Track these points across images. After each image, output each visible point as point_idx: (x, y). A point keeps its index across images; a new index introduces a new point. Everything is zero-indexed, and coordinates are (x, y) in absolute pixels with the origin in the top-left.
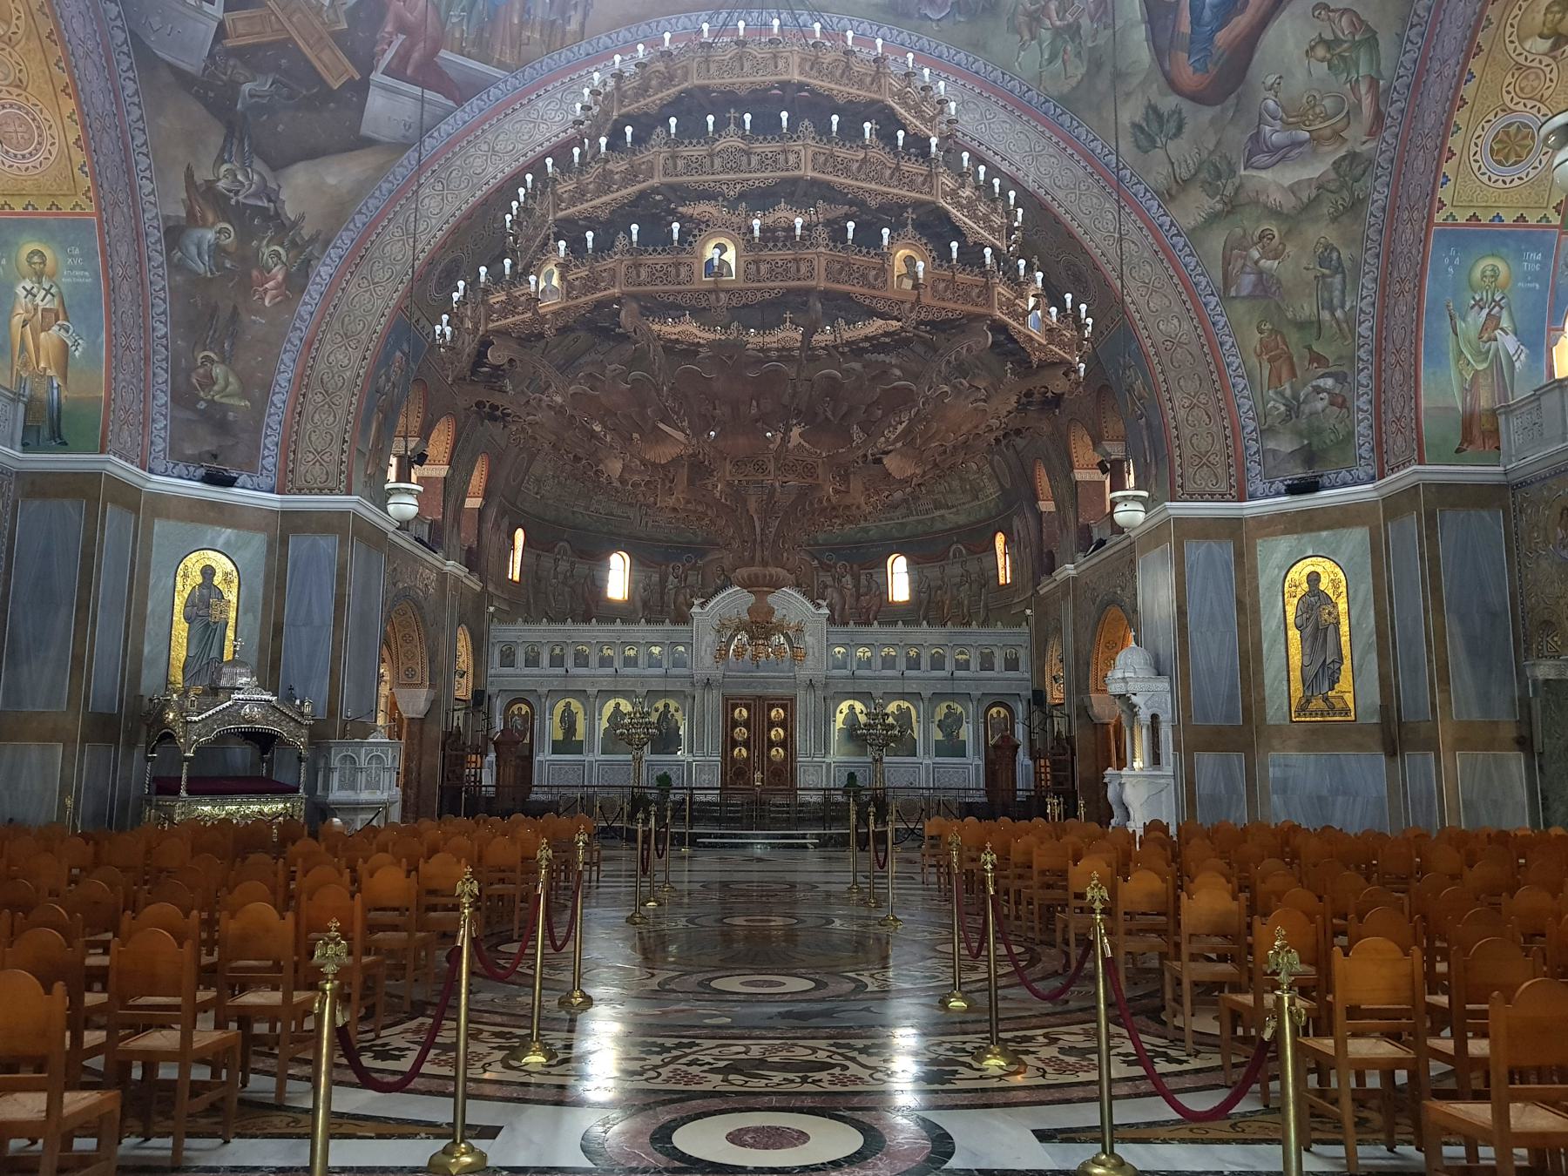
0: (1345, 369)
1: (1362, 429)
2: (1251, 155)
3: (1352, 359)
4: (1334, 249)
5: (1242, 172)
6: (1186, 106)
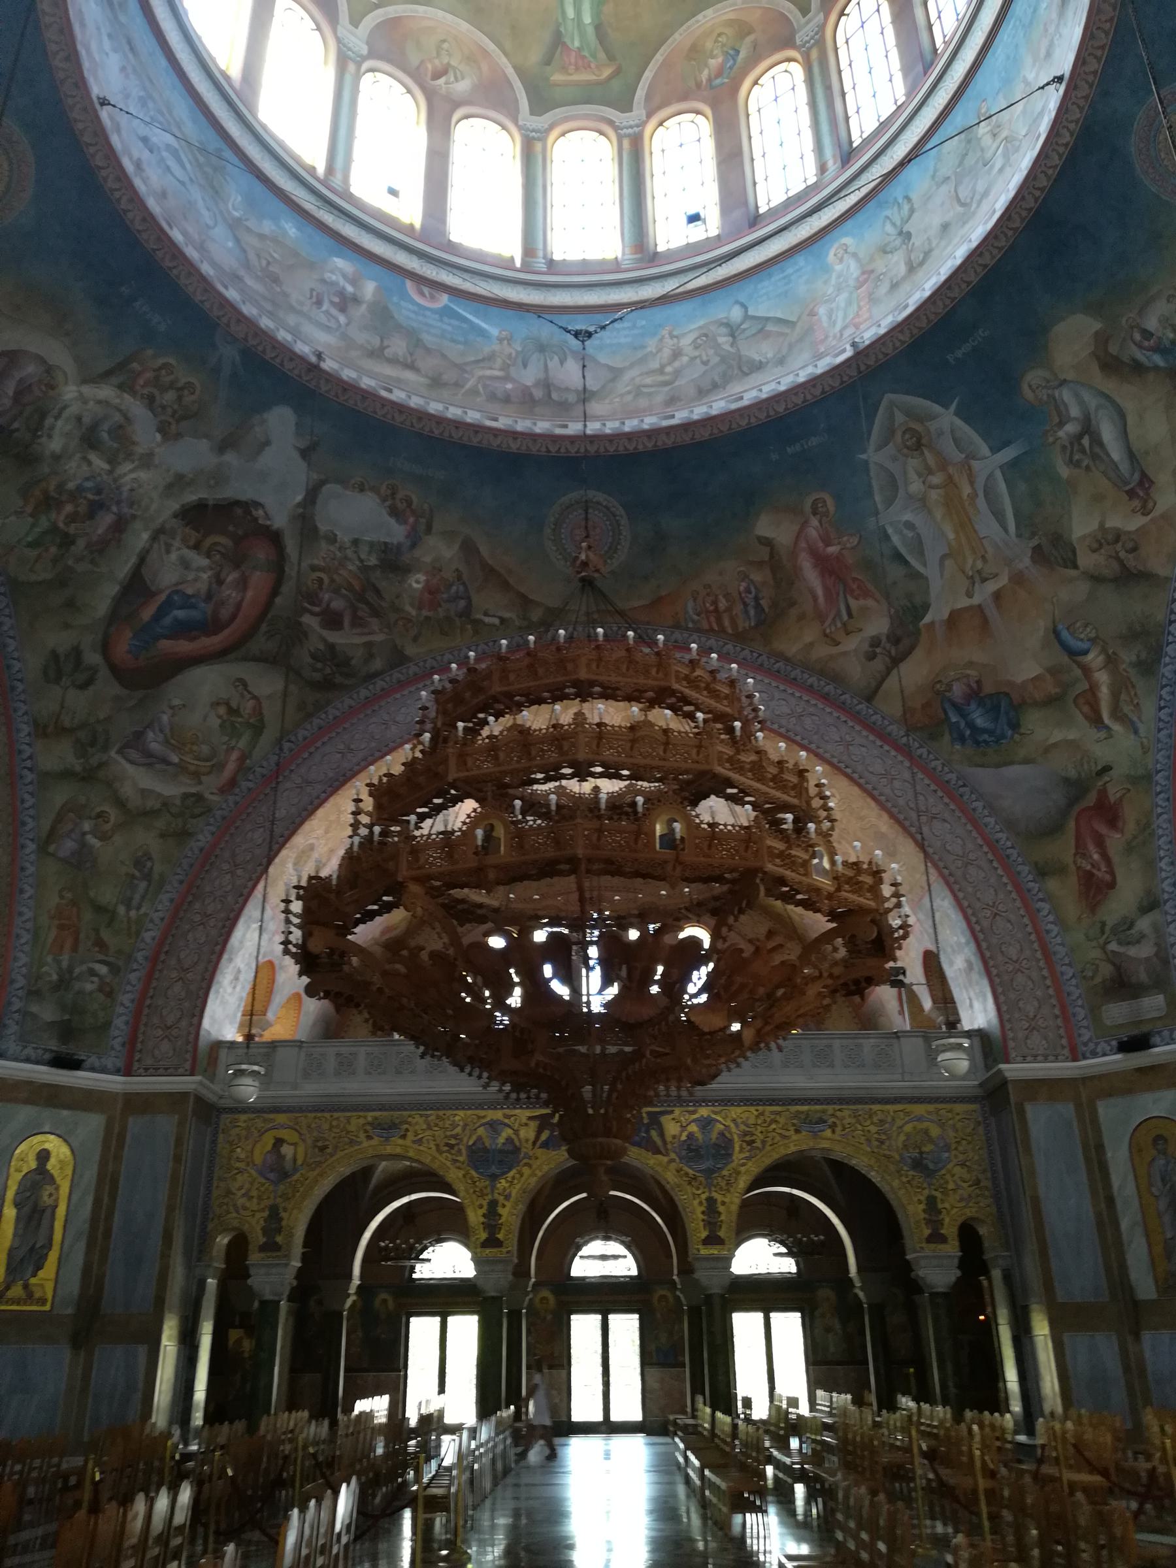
2: (127, 746)
4: (150, 859)
5: (113, 754)
6: (104, 672)
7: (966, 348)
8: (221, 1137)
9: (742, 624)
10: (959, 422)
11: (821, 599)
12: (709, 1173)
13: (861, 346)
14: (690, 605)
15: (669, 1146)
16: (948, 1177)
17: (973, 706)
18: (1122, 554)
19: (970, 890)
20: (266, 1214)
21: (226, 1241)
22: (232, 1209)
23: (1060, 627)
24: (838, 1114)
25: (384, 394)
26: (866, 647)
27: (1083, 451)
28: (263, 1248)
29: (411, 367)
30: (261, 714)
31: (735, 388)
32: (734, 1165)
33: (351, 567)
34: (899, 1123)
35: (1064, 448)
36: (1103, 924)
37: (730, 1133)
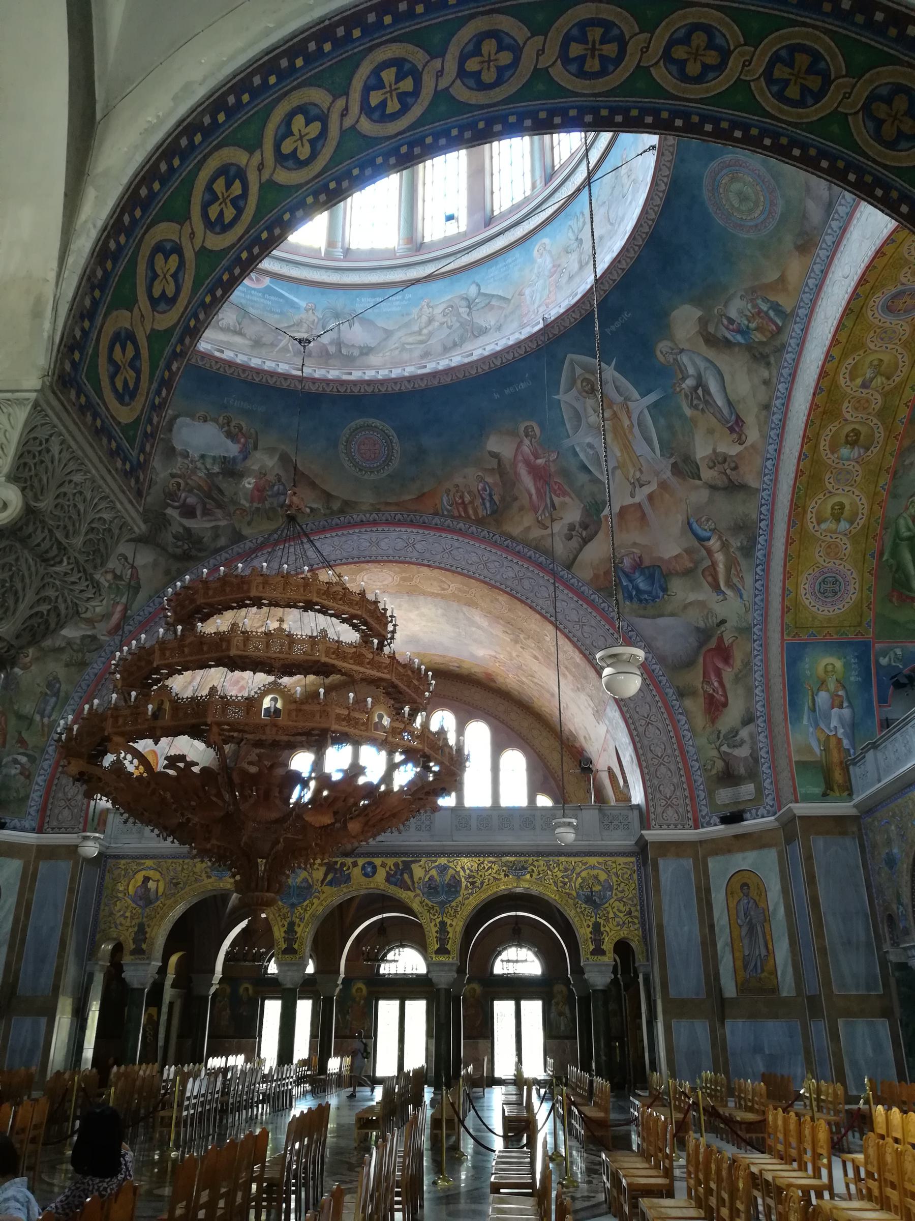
0: (36, 755)
1: (35, 796)
3: (43, 751)
4: (59, 682)
7: (618, 324)
8: (107, 875)
9: (482, 513)
10: (617, 374)
11: (534, 497)
12: (442, 904)
13: (549, 321)
14: (445, 499)
15: (416, 885)
16: (610, 909)
17: (637, 574)
18: (728, 471)
19: (632, 705)
20: (136, 929)
21: (110, 947)
22: (113, 926)
23: (692, 520)
24: (535, 863)
25: (217, 354)
26: (566, 531)
27: (698, 398)
28: (133, 953)
29: (240, 333)
30: (138, 578)
31: (468, 347)
32: (460, 898)
33: (200, 474)
34: (578, 870)
35: (686, 396)
36: (719, 732)
37: (459, 876)
